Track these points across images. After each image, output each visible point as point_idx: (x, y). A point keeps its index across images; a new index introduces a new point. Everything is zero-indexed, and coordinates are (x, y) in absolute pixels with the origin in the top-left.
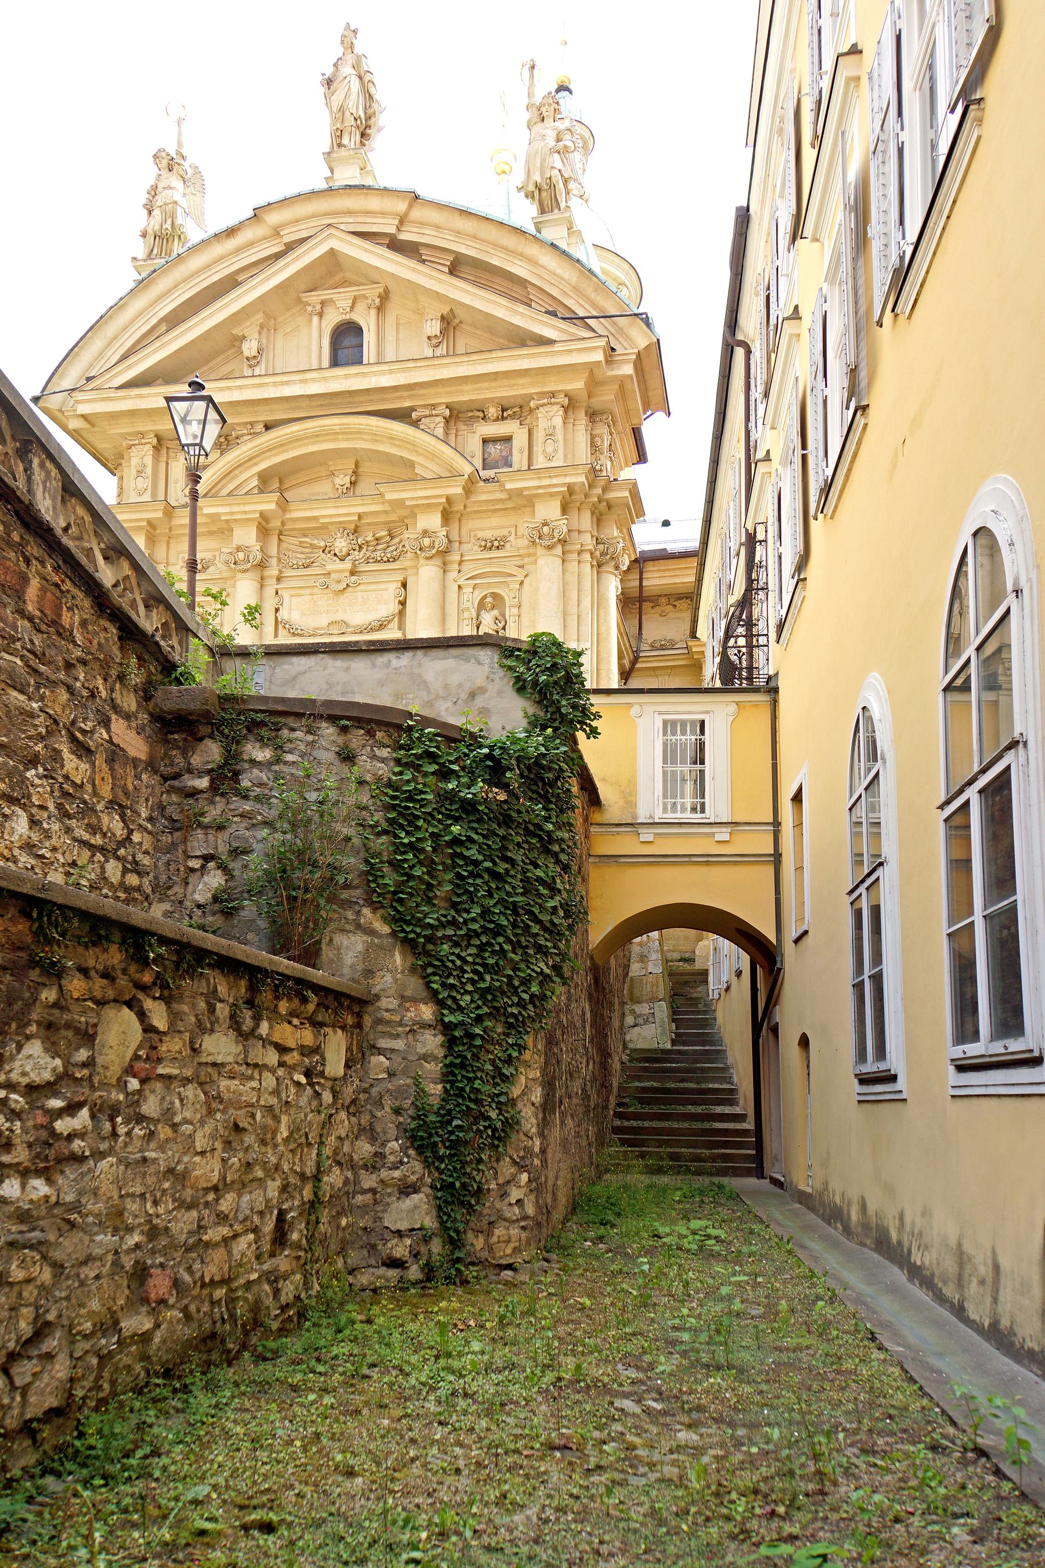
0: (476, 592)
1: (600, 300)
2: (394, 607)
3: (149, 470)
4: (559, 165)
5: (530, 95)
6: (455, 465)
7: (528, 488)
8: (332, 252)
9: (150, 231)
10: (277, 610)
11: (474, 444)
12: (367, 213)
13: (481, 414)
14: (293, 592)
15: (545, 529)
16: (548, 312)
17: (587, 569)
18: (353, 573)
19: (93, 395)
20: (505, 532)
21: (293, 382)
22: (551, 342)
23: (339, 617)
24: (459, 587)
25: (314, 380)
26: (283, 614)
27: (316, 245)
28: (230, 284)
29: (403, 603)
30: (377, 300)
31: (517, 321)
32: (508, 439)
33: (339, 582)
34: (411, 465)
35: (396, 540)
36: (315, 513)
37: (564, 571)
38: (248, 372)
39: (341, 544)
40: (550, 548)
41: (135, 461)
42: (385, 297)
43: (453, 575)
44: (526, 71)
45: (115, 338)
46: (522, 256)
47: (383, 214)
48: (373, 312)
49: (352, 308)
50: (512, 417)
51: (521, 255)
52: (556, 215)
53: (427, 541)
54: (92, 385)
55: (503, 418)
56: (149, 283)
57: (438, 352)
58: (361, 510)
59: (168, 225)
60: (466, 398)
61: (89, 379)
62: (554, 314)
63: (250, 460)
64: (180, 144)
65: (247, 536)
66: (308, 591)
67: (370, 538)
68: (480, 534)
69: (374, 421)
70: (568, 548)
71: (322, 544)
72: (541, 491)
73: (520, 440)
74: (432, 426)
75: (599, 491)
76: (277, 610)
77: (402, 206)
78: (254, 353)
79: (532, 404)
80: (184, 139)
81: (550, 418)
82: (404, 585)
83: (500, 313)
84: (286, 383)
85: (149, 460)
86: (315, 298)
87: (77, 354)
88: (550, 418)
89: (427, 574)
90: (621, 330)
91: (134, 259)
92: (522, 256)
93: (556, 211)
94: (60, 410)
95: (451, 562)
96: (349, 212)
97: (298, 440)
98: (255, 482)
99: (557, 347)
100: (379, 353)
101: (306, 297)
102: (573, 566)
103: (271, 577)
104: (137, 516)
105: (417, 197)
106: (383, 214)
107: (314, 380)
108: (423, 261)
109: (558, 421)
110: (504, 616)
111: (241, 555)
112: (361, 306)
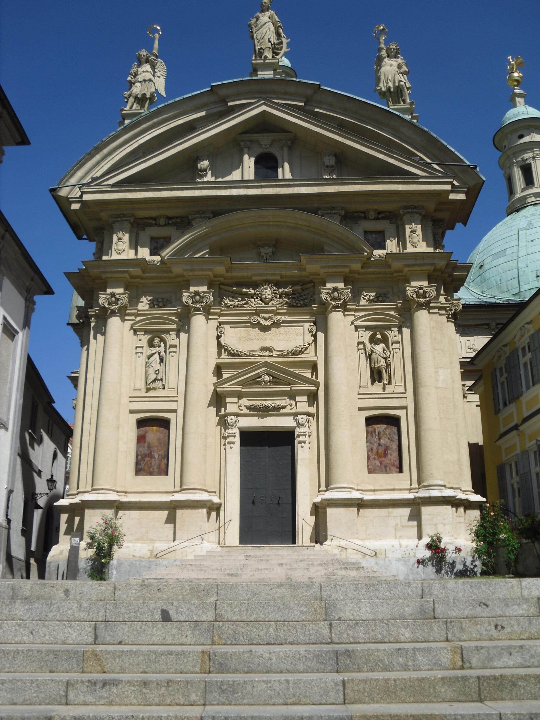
8: (264, 111)
13: (363, 215)
15: (421, 291)
22: (417, 176)
23: (267, 344)
30: (289, 143)
33: (266, 319)
48: (286, 149)
49: (271, 145)
50: (383, 218)
55: (377, 219)
76: (218, 337)
77: (309, 92)
86: (247, 137)
93: (402, 103)
110: (388, 348)
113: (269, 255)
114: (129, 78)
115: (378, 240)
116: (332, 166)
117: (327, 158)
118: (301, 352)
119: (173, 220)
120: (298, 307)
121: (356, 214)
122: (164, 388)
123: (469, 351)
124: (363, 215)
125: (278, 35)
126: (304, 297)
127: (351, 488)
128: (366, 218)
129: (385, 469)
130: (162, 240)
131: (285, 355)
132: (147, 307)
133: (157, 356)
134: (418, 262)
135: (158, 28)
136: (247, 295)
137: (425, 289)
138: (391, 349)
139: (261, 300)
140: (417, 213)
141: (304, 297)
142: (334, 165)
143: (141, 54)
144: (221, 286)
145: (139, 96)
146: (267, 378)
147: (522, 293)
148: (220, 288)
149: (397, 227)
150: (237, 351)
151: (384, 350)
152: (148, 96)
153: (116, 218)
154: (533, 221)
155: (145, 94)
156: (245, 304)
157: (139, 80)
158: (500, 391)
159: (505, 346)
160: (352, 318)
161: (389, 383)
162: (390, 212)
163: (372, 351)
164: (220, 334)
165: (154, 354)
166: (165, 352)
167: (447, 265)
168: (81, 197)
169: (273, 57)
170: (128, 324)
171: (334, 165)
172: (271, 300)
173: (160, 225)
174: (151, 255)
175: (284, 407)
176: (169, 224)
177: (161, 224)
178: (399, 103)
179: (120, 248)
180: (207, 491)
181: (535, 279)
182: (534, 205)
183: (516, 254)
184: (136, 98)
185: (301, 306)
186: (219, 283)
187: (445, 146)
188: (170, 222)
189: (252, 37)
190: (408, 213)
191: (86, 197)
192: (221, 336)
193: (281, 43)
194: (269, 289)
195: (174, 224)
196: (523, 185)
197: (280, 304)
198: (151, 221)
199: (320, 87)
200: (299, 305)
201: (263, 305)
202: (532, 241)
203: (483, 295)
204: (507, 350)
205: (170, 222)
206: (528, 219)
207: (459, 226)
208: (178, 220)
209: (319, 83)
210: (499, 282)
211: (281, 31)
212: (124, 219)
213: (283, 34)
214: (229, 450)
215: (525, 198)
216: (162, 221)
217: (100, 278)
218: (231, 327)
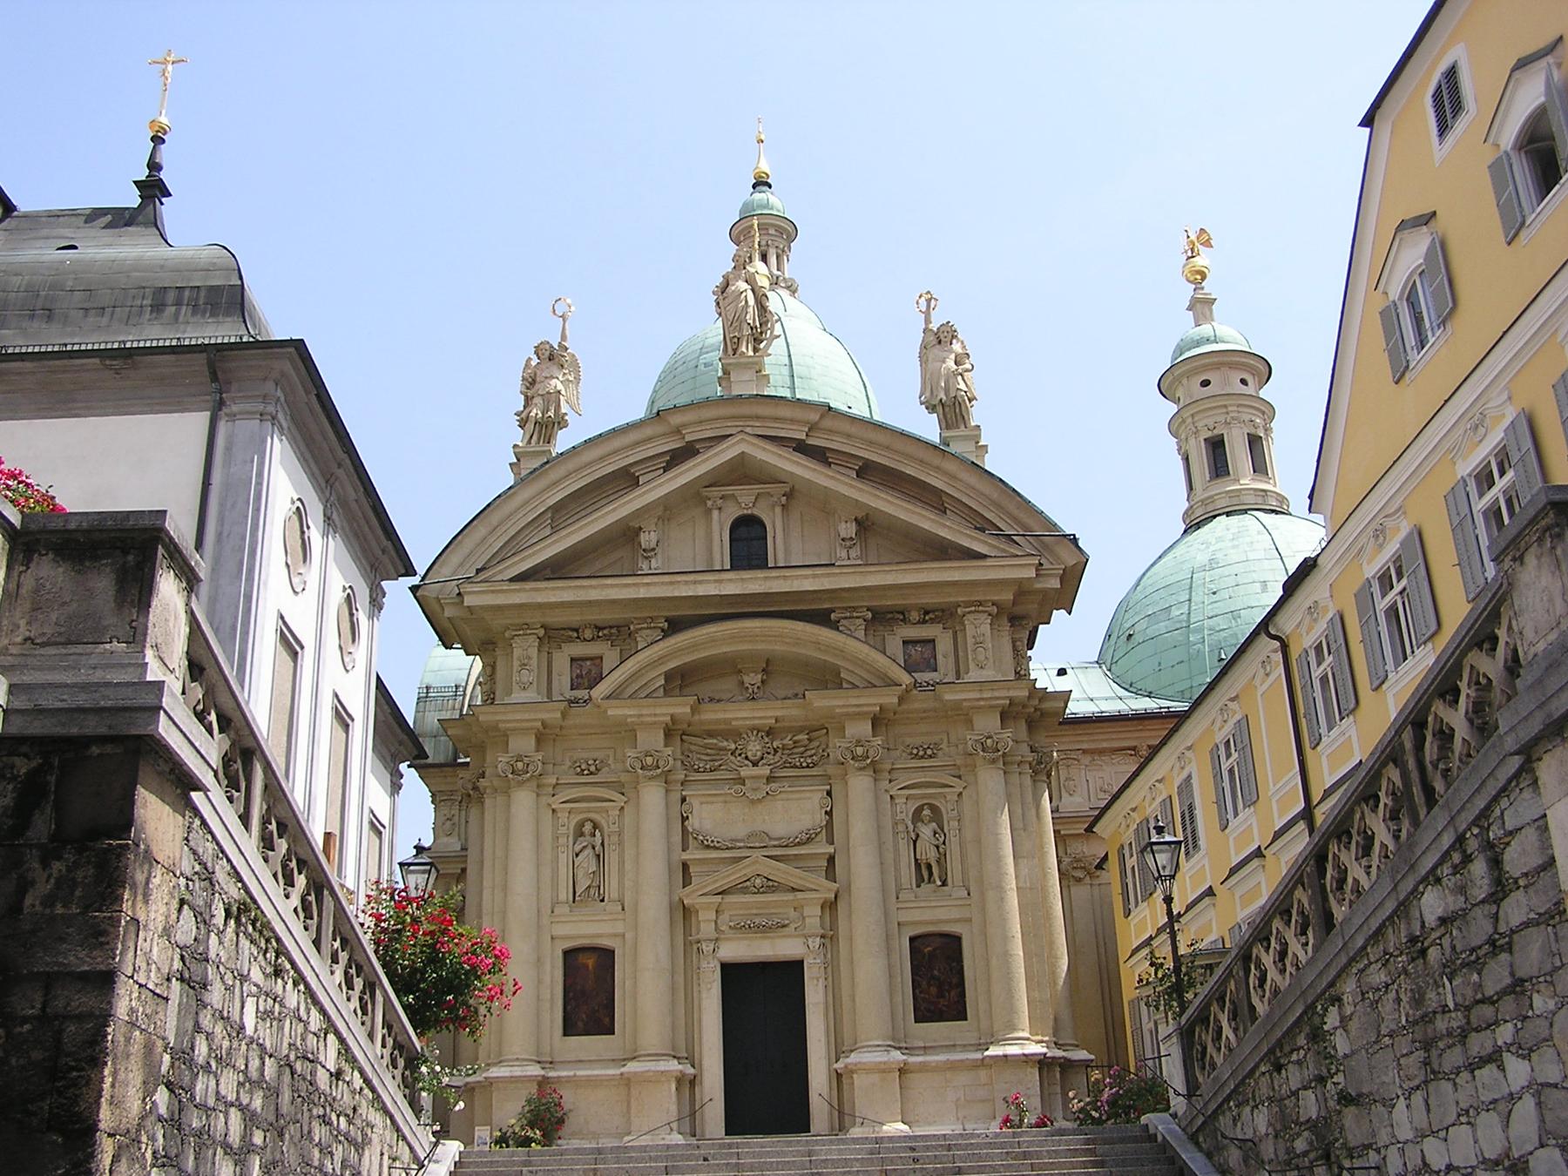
0: (910, 803)
1: (1022, 516)
2: (821, 818)
3: (534, 662)
4: (962, 386)
5: (928, 321)
6: (890, 674)
7: (969, 700)
8: (743, 452)
10: (684, 819)
11: (894, 644)
12: (776, 419)
13: (901, 617)
14: (704, 799)
15: (989, 741)
16: (976, 528)
17: (1028, 781)
18: (770, 779)
19: (483, 587)
20: (936, 739)
21: (708, 582)
22: (985, 556)
23: (759, 826)
24: (891, 796)
25: (730, 580)
26: (693, 823)
28: (627, 479)
29: (829, 813)
31: (943, 533)
34: (836, 672)
35: (816, 744)
36: (729, 715)
37: (1006, 783)
38: (645, 566)
39: (754, 748)
40: (994, 761)
41: (517, 652)
42: (790, 495)
43: (885, 784)
44: (923, 301)
46: (938, 469)
47: (792, 421)
48: (778, 510)
50: (932, 621)
51: (938, 468)
52: (962, 431)
53: (860, 751)
54: (482, 576)
55: (925, 622)
56: (540, 474)
57: (853, 553)
58: (779, 713)
59: (551, 413)
60: (889, 603)
61: (478, 571)
62: (983, 530)
63: (661, 660)
64: (564, 337)
65: (652, 740)
66: (721, 799)
67: (785, 742)
68: (909, 741)
69: (800, 626)
70: (1009, 759)
71: (733, 746)
72: (982, 703)
73: (944, 644)
74: (852, 628)
75: (1036, 702)
76: (684, 819)
77: (814, 417)
78: (653, 545)
79: (959, 610)
80: (567, 332)
81: (978, 627)
82: (829, 793)
83: (926, 525)
84: (701, 582)
85: (534, 652)
86: (715, 492)
87: (461, 542)
88: (978, 627)
89: (860, 786)
90: (1046, 546)
91: (515, 446)
92: (938, 469)
93: (963, 427)
94: (438, 599)
95: (881, 771)
96: (758, 418)
97: (713, 641)
99: (989, 562)
100: (787, 551)
101: (706, 492)
102: (1015, 778)
103: (676, 781)
104: (533, 716)
105: (830, 408)
106: (792, 421)
108: (830, 464)
109: (986, 628)
111: (649, 760)
112: (762, 503)
115: (926, 656)
116: (851, 539)
117: (843, 525)
118: (809, 840)
119: (606, 632)
121: (890, 616)
122: (602, 901)
123: (1102, 795)
126: (813, 751)
127: (889, 1046)
128: (904, 620)
129: (941, 1017)
130: (588, 663)
131: (786, 846)
133: (589, 851)
134: (985, 696)
136: (724, 749)
138: (946, 831)
139: (747, 758)
140: (982, 612)
141: (813, 751)
142: (854, 536)
144: (684, 737)
146: (758, 881)
147: (1194, 689)
148: (682, 740)
149: (955, 633)
150: (712, 841)
151: (935, 833)
153: (516, 630)
154: (1219, 555)
156: (720, 765)
157: (540, 392)
158: (1130, 880)
159: (1133, 810)
161: (944, 884)
162: (943, 611)
163: (918, 836)
165: (584, 847)
166: (603, 844)
167: (1029, 697)
168: (459, 594)
169: (755, 350)
170: (544, 800)
171: (854, 536)
172: (762, 758)
175: (784, 926)
176: (598, 637)
177: (586, 636)
179: (525, 679)
180: (674, 1057)
182: (1228, 514)
185: (808, 767)
186: (681, 732)
188: (600, 634)
190: (969, 612)
191: (468, 601)
192: (687, 817)
195: (607, 638)
198: (571, 633)
200: (804, 764)
201: (750, 764)
202: (1214, 593)
203: (1131, 689)
204: (1137, 818)
205: (600, 634)
206: (1212, 548)
207: (1058, 615)
208: (614, 631)
212: (529, 632)
214: (704, 995)
216: (588, 634)
217: (496, 728)
218: (702, 803)
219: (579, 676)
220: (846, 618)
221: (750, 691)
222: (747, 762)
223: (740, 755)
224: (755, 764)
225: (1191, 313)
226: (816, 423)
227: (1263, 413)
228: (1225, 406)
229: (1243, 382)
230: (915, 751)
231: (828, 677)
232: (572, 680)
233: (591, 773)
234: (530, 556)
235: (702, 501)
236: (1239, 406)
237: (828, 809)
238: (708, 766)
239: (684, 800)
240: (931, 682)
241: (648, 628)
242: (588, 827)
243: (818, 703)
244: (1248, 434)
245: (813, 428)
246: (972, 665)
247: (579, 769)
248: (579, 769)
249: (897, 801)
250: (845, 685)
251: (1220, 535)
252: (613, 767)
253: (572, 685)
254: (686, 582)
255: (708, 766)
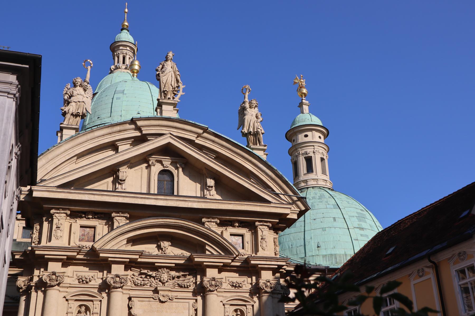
9: (71, 112)
15: (269, 284)
22: (269, 202)
24: (224, 305)
25: (161, 199)
27: (163, 139)
29: (196, 310)
32: (242, 236)
45: (51, 160)
66: (148, 299)
76: (130, 308)
82: (196, 300)
93: (258, 145)
98: (125, 242)
99: (272, 205)
107: (161, 199)
113: (166, 248)
114: (66, 97)
116: (212, 187)
120: (185, 287)
124: (230, 224)
125: (177, 81)
130: (88, 229)
132: (77, 282)
135: (91, 62)
136: (150, 276)
137: (271, 282)
139: (160, 281)
140: (266, 226)
143: (77, 80)
145: (74, 114)
152: (81, 114)
154: (315, 204)
155: (79, 113)
157: (75, 101)
160: (221, 299)
164: (130, 306)
172: (167, 282)
173: (89, 218)
174: (80, 241)
178: (256, 144)
181: (316, 248)
183: (303, 228)
184: (72, 114)
185: (187, 287)
187: (287, 182)
189: (159, 80)
192: (131, 308)
193: (178, 87)
194: (166, 274)
195: (99, 218)
196: (305, 172)
197: (172, 284)
199: (207, 129)
201: (161, 284)
202: (315, 219)
208: (102, 216)
209: (207, 127)
210: (291, 247)
211: (179, 78)
213: (180, 81)
215: (306, 181)
219: (83, 235)
220: (208, 222)
221: (164, 250)
222: (160, 283)
223: (157, 279)
224: (163, 283)
225: (300, 108)
226: (201, 134)
227: (325, 150)
228: (313, 146)
229: (320, 137)
230: (234, 284)
231: (201, 249)
232: (80, 236)
233: (87, 283)
234: (68, 176)
235: (146, 161)
236: (319, 146)
237: (196, 308)
238: (142, 283)
239: (130, 299)
240: (242, 254)
241: (119, 216)
242: (83, 309)
243: (196, 260)
244: (321, 157)
245: (199, 135)
246: (260, 248)
247: (81, 280)
248: (81, 280)
249: (226, 306)
250: (207, 253)
251: (313, 196)
252: (97, 280)
253: (80, 239)
254: (142, 198)
255: (142, 283)
